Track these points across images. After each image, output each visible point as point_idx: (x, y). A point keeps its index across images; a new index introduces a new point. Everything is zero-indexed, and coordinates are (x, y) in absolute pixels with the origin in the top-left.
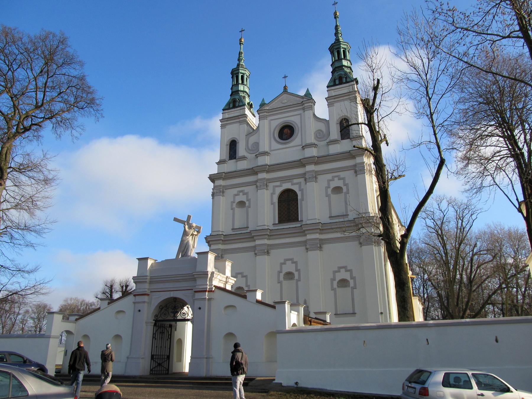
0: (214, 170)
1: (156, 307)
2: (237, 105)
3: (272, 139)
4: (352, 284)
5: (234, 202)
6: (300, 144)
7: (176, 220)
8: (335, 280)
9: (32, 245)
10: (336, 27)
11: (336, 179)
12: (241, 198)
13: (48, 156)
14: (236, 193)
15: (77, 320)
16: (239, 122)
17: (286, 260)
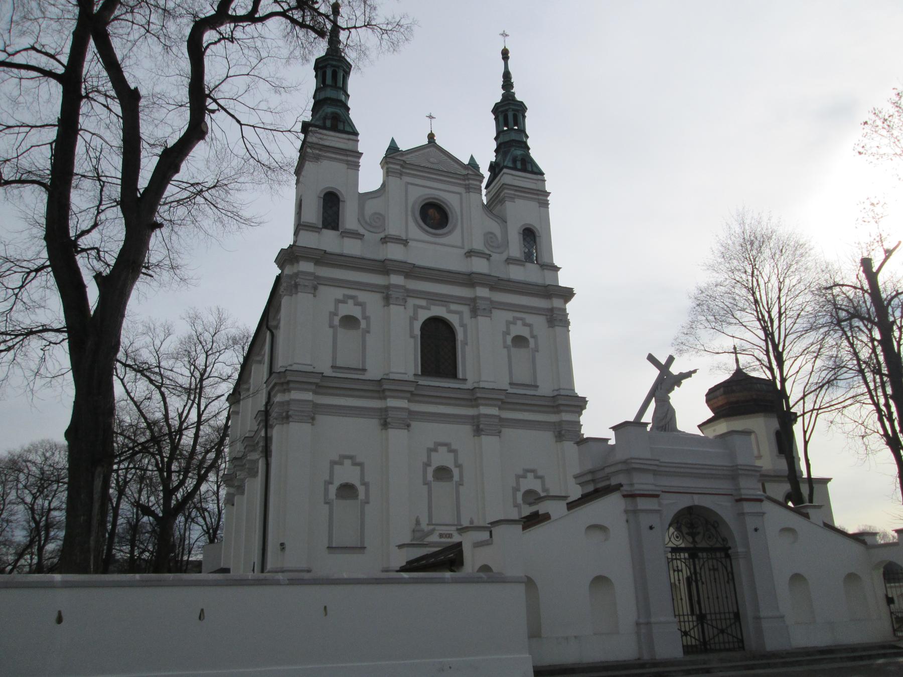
3: (410, 218)
5: (334, 314)
6: (459, 244)
8: (518, 490)
10: (507, 76)
11: (519, 323)
14: (341, 297)
17: (438, 444)
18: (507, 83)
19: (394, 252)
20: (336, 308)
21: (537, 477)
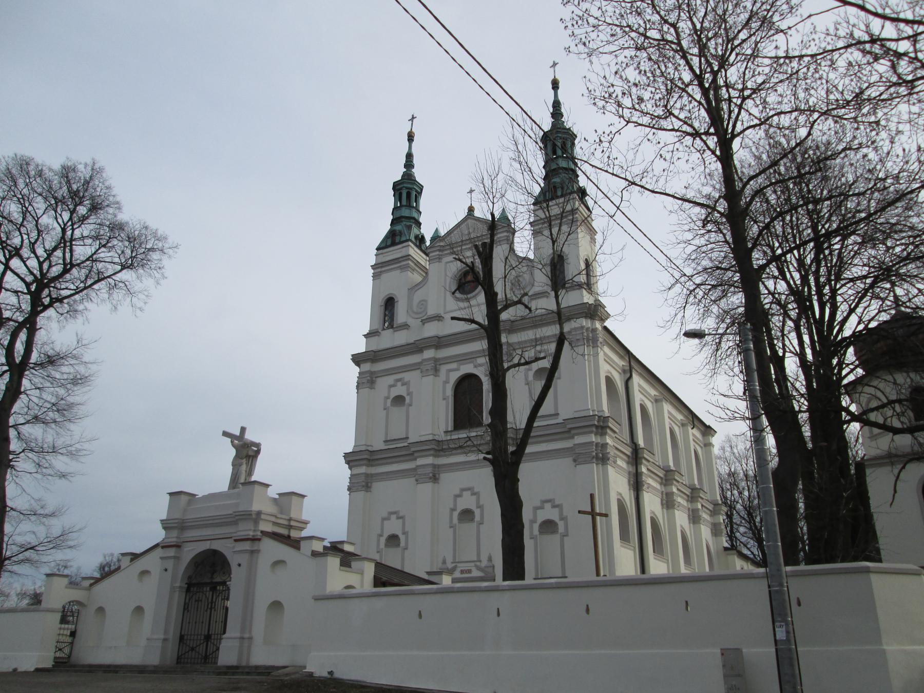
0: (361, 347)
1: (189, 564)
2: (397, 241)
4: (561, 528)
5: (387, 398)
9: (63, 476)
12: (400, 390)
13: (84, 342)
14: (392, 383)
15: (91, 585)
16: (400, 268)
17: (463, 490)
18: (557, 112)
19: (432, 330)
20: (389, 392)
21: (554, 506)
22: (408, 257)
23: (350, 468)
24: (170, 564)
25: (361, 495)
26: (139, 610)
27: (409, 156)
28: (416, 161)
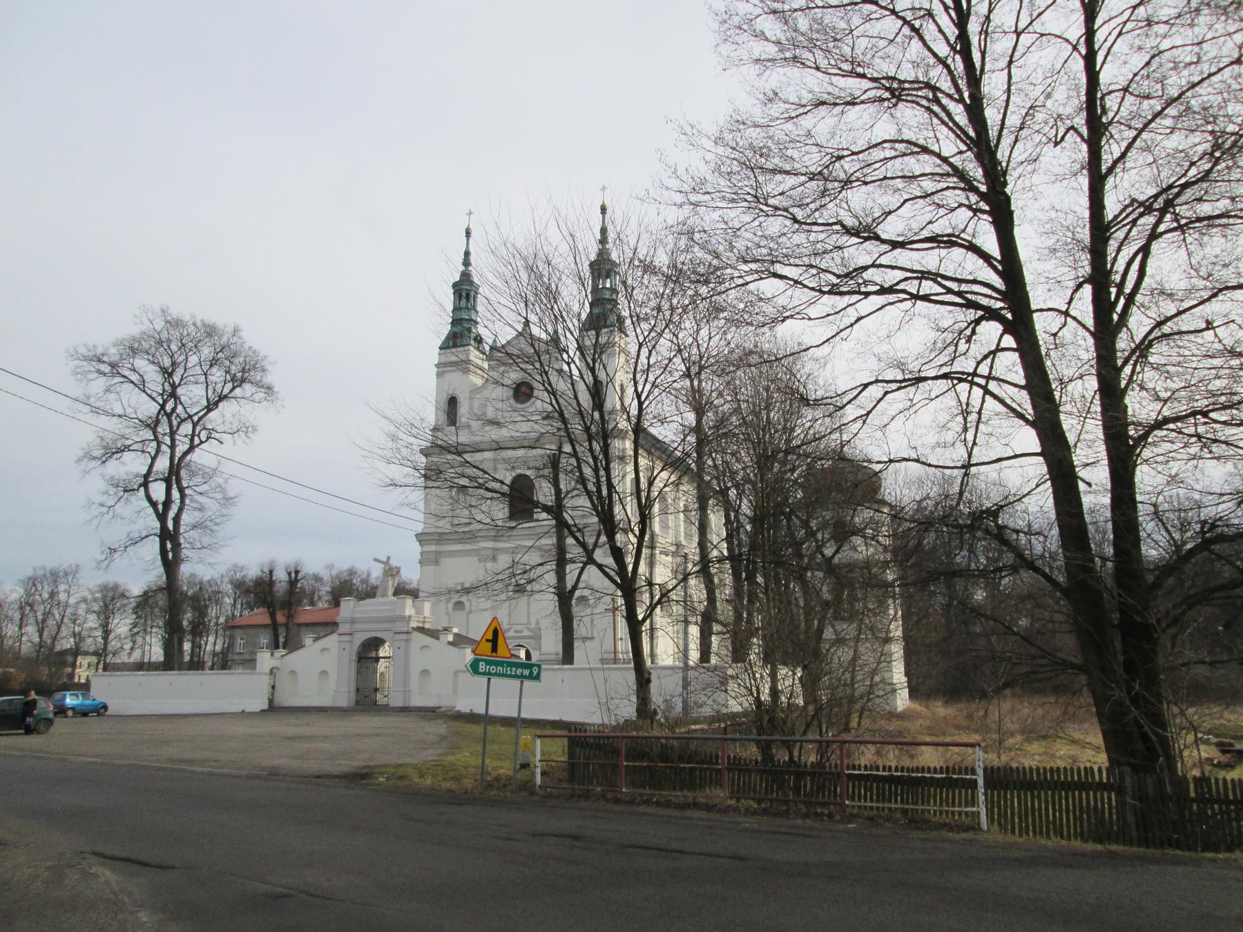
7: (376, 560)
22: (468, 362)
23: (421, 545)
24: (347, 646)
25: (432, 568)
26: (324, 673)
27: (467, 254)
28: (472, 259)
